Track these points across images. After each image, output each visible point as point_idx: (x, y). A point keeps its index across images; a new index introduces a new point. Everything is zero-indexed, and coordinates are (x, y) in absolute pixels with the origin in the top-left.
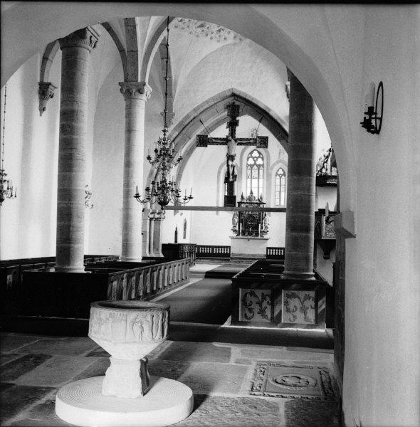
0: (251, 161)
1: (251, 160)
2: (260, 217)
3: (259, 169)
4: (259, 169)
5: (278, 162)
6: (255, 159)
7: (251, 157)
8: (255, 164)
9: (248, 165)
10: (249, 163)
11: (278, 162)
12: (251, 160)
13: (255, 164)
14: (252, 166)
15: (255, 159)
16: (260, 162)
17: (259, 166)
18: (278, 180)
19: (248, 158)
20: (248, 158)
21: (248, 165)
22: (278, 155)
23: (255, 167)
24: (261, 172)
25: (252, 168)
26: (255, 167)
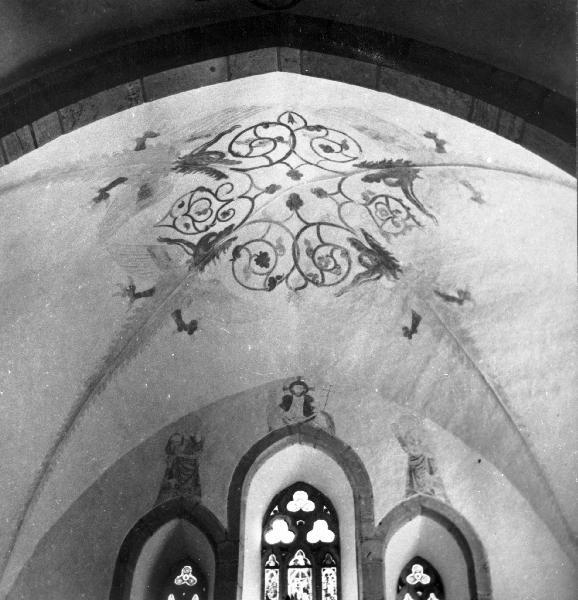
0: (281, 533)
5: (402, 513)
7: (284, 513)
8: (300, 542)
9: (266, 549)
10: (272, 538)
11: (402, 513)
14: (283, 553)
15: (301, 523)
16: (320, 533)
19: (266, 524)
20: (266, 524)
21: (266, 549)
22: (403, 475)
23: (300, 558)
26: (300, 558)
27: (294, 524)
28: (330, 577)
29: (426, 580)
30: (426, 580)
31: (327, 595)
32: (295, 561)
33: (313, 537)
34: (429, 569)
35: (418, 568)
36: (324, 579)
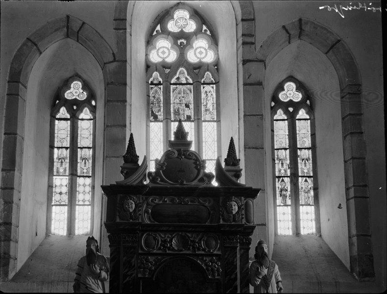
1: (163, 44)
2: (229, 268)
3: (197, 85)
4: (197, 85)
6: (182, 40)
7: (165, 32)
8: (182, 61)
9: (149, 67)
12: (163, 44)
13: (182, 61)
15: (182, 40)
17: (197, 70)
18: (281, 129)
19: (150, 41)
21: (149, 67)
23: (183, 75)
24: (209, 93)
25: (167, 78)
27: (175, 43)
28: (209, 94)
29: (298, 97)
30: (298, 97)
31: (206, 110)
32: (178, 79)
33: (192, 57)
34: (300, 87)
35: (290, 86)
36: (203, 96)
